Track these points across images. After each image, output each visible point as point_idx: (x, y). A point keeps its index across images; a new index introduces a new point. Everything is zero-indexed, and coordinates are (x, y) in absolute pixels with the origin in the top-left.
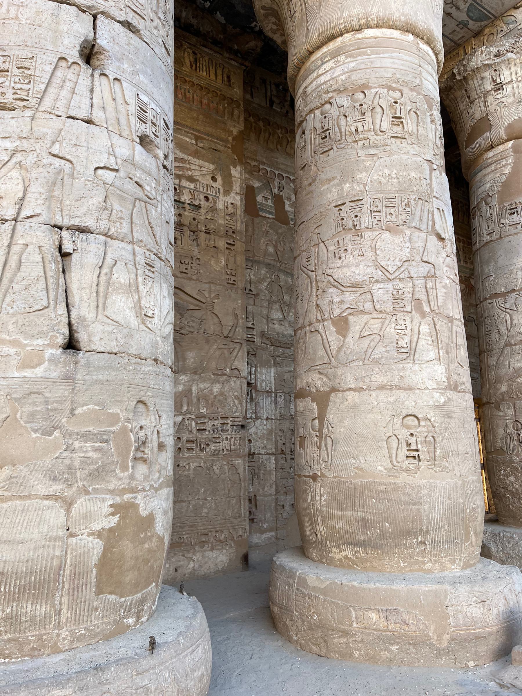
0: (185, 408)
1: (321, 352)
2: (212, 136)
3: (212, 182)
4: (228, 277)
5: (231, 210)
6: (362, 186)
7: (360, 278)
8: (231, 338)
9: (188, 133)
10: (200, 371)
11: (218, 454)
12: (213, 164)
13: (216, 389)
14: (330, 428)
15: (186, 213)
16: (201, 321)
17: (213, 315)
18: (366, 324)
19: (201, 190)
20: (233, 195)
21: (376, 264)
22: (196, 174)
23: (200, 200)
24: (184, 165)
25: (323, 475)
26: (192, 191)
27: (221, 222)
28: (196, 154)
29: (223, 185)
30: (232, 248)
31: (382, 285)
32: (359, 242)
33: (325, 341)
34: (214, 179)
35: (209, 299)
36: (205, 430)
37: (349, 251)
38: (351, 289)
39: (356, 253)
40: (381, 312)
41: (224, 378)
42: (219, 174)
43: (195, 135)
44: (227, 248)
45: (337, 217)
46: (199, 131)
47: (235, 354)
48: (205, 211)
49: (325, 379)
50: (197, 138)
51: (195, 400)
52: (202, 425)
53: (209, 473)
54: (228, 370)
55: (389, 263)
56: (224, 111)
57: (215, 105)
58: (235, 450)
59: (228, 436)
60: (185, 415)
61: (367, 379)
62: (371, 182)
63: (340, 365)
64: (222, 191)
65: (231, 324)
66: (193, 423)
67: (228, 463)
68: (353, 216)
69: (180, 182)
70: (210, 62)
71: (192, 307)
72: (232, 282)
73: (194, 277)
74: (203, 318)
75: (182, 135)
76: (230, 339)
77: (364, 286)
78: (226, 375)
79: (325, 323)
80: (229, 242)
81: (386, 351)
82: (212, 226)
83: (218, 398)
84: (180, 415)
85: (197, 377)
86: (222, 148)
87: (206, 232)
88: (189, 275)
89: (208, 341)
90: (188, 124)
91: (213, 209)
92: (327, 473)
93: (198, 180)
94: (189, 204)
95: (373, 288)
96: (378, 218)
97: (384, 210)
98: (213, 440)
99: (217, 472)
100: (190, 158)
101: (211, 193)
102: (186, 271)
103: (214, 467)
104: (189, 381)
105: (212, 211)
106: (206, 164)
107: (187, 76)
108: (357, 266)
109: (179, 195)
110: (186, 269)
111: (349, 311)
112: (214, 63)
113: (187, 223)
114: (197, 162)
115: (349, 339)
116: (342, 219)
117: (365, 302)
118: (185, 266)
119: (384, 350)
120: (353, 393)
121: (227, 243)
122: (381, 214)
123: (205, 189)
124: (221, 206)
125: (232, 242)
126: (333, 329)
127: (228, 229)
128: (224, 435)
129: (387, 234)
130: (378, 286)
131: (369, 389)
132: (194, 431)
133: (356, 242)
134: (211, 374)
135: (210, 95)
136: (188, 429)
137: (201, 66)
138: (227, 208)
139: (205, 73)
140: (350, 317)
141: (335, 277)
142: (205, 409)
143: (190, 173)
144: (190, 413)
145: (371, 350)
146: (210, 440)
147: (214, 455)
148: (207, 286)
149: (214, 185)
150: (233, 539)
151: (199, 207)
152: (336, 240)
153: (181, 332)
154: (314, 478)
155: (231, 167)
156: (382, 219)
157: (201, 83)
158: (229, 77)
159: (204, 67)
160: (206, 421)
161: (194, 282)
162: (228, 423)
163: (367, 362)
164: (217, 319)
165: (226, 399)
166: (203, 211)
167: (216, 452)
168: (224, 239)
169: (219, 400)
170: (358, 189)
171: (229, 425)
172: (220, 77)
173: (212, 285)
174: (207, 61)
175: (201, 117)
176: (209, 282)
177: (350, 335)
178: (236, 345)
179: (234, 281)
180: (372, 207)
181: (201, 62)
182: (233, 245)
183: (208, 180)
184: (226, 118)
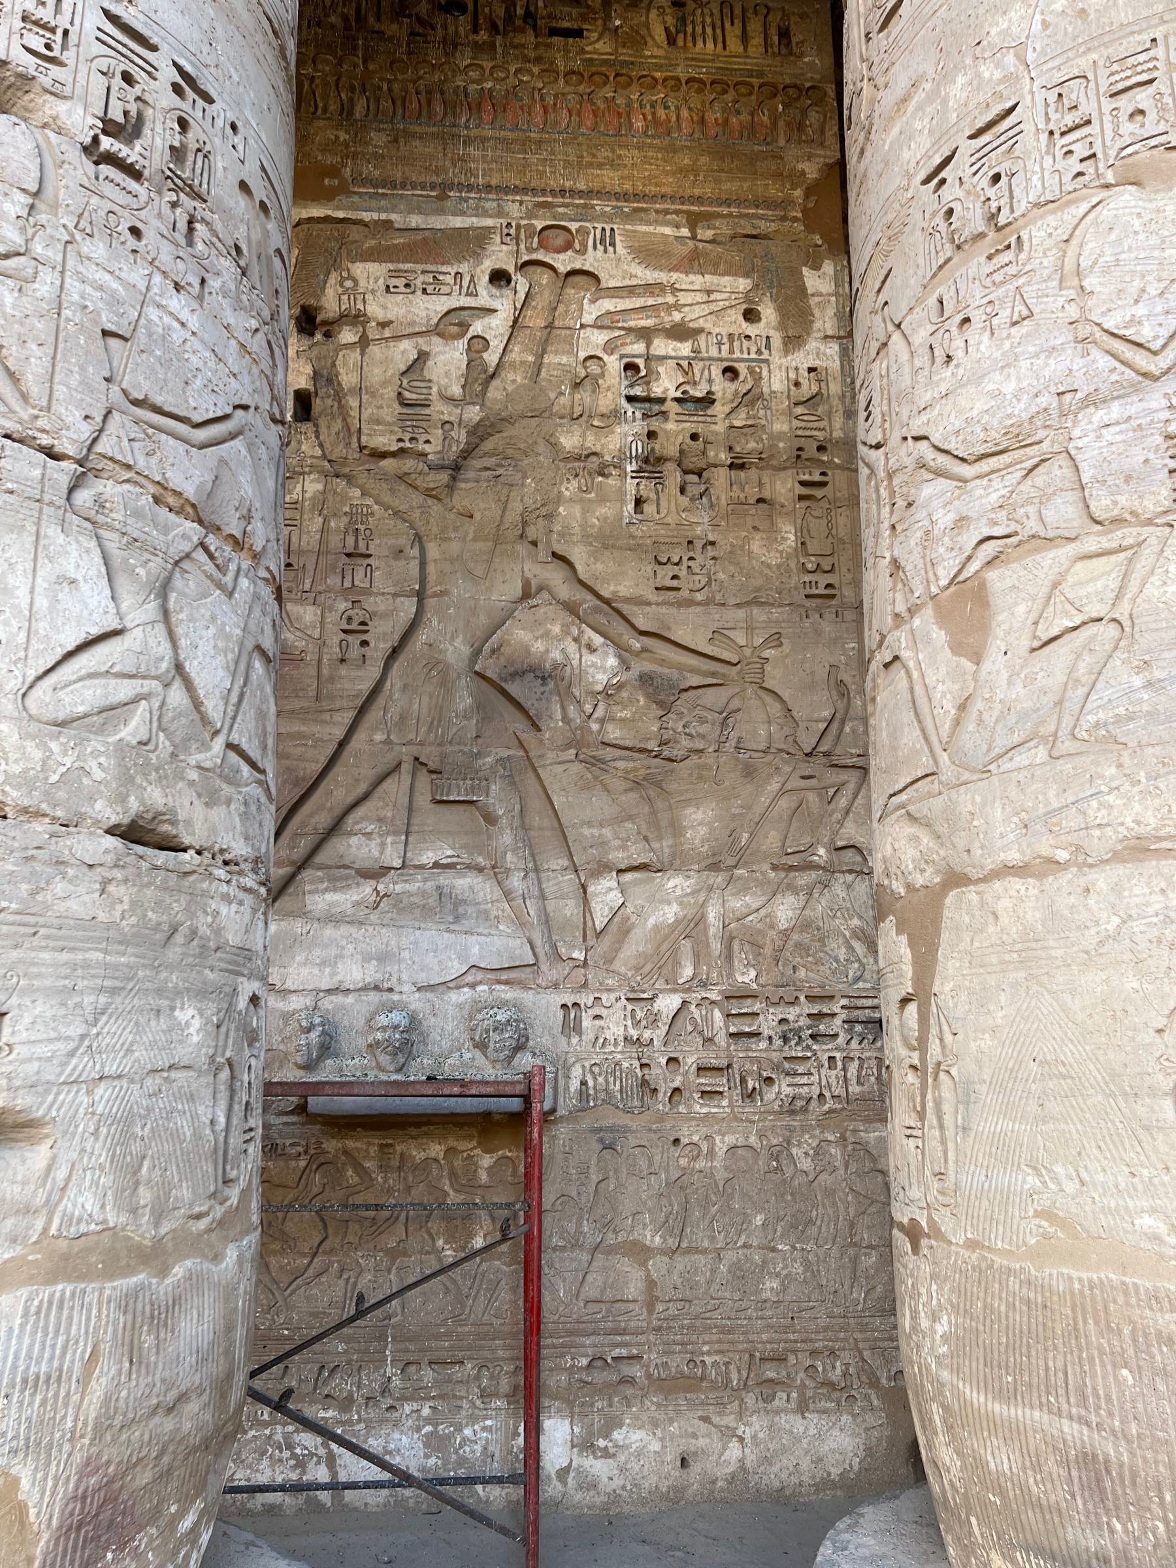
0: (688, 972)
1: (910, 737)
2: (741, 202)
3: (744, 324)
4: (807, 578)
5: (809, 387)
6: (1010, 59)
7: (1021, 410)
8: (827, 754)
9: (667, 212)
10: (731, 861)
11: (804, 1110)
12: (746, 275)
13: (785, 911)
14: (948, 1038)
15: (671, 426)
16: (726, 717)
17: (761, 693)
18: (1055, 585)
19: (714, 352)
20: (813, 344)
21: (1084, 330)
22: (694, 315)
23: (710, 381)
24: (660, 300)
25: (936, 1232)
26: (685, 364)
27: (780, 426)
28: (694, 262)
29: (782, 326)
30: (818, 493)
31: (1116, 410)
32: (1012, 270)
33: (919, 690)
34: (751, 315)
35: (748, 652)
36: (756, 1035)
37: (977, 317)
38: (993, 462)
39: (1005, 314)
40: (1118, 522)
41: (814, 875)
42: (767, 299)
43: (689, 214)
44: (801, 498)
45: (934, 214)
46: (699, 200)
47: (843, 802)
48: (727, 409)
49: (926, 840)
50: (694, 221)
51: (716, 946)
52: (748, 1020)
53: (779, 1169)
54: (822, 851)
55: (1141, 311)
56: (775, 124)
57: (745, 117)
58: (863, 1098)
59: (838, 1055)
60: (689, 990)
61: (1072, 820)
62: (1045, 25)
63: (967, 776)
64: (777, 342)
65: (827, 713)
66: (717, 1015)
67: (843, 1138)
68: (985, 182)
69: (648, 347)
70: (726, 11)
71: (695, 681)
72: (821, 591)
73: (699, 597)
74: (732, 706)
75: (649, 223)
76: (824, 760)
77: (1041, 434)
78: (817, 867)
79: (917, 622)
80: (807, 477)
81: (1149, 684)
82: (752, 445)
83: (795, 937)
84: (675, 991)
85: (720, 879)
86: (773, 227)
87: (731, 466)
88: (685, 593)
89: (749, 772)
90: (664, 190)
91: (751, 398)
92: (946, 1225)
93: (700, 331)
94: (677, 400)
95: (1076, 433)
96: (1081, 150)
97: (1107, 105)
98: (787, 1065)
99: (806, 1164)
100: (675, 276)
101: (742, 354)
102: (675, 583)
103: (794, 1151)
104: (692, 893)
105: (752, 403)
106: (726, 280)
107: (659, 67)
108: (1008, 363)
109: (648, 383)
110: (674, 577)
111: (990, 548)
112: (738, 11)
113: (672, 450)
114: (697, 281)
115: (994, 662)
116: (950, 212)
117: (1045, 497)
118: (671, 570)
119: (1137, 681)
120: (1016, 884)
121: (803, 483)
122: (1094, 129)
123: (725, 348)
124: (776, 382)
125: (817, 477)
126: (939, 636)
127: (802, 442)
128: (823, 1050)
129: (1127, 196)
130: (1100, 416)
131: (1082, 860)
132: (722, 1039)
133: (998, 277)
134: (766, 867)
135: (730, 97)
136: (701, 1033)
137: (699, 29)
138: (797, 384)
139: (710, 45)
140: (992, 575)
141: (936, 438)
142: (753, 974)
143: (677, 316)
144: (704, 985)
145: (1081, 691)
146: (777, 1067)
147: (792, 1112)
148: (741, 613)
149: (751, 330)
150: (874, 1383)
151: (708, 401)
152: (932, 301)
153: (666, 753)
154: (914, 1233)
155: (805, 270)
156: (1098, 148)
157: (702, 73)
158: (784, 34)
159: (709, 30)
160: (757, 1007)
161: (699, 609)
162: (834, 1015)
163: (1066, 746)
164: (777, 705)
165: (821, 940)
166: (719, 409)
167: (799, 1103)
168: (789, 472)
169: (798, 945)
170: (998, 75)
171: (838, 1021)
172: (757, 41)
173: (756, 610)
174: (716, 11)
175: (704, 160)
176: (748, 603)
177: (996, 645)
178: (844, 776)
179: (828, 586)
180: (1054, 116)
181: (699, 20)
182: (823, 484)
183: (735, 322)
184: (782, 143)
